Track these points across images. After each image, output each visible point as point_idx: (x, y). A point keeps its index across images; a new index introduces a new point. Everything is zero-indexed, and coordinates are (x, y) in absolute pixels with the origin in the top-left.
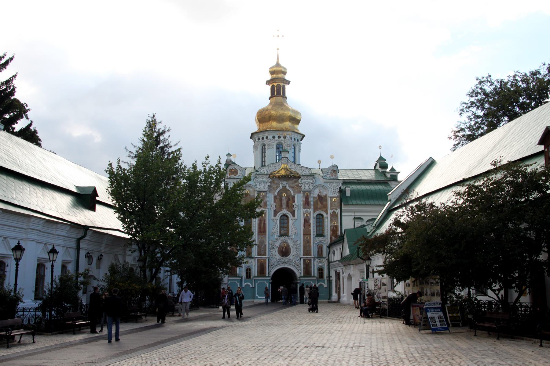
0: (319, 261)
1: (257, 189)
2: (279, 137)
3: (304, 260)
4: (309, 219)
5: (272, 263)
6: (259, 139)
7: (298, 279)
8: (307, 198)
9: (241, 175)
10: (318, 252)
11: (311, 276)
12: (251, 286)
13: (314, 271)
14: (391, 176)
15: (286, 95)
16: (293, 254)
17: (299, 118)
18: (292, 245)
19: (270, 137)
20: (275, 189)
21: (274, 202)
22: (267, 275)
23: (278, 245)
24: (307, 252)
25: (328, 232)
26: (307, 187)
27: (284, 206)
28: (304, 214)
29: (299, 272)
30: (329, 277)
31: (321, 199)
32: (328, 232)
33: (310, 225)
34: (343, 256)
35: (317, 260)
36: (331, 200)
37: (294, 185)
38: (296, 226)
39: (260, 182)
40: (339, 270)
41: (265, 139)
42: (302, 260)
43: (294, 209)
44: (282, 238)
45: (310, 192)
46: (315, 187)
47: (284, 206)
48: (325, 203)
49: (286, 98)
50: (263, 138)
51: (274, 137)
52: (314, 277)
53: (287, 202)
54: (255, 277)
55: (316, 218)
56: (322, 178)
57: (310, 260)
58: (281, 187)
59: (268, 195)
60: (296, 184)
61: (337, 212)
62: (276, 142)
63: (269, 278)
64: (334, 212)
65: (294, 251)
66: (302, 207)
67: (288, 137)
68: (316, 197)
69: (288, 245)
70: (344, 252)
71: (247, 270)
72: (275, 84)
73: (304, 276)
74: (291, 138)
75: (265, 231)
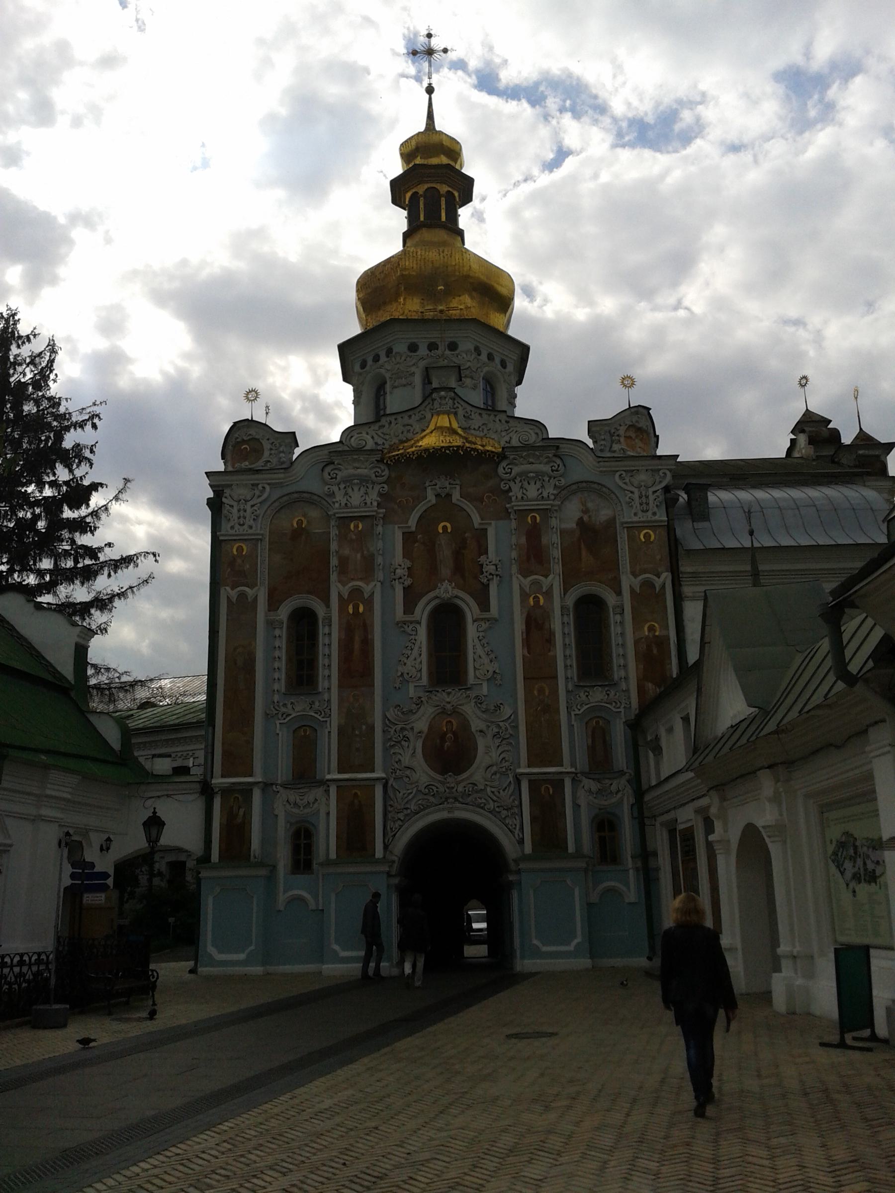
0: (594, 786)
2: (432, 347)
3: (534, 785)
6: (363, 365)
7: (513, 866)
8: (534, 534)
9: (274, 461)
10: (592, 749)
12: (312, 906)
13: (577, 830)
17: (503, 291)
18: (482, 726)
19: (401, 348)
21: (407, 554)
22: (379, 853)
23: (421, 724)
24: (544, 749)
25: (626, 664)
26: (532, 491)
27: (446, 571)
28: (524, 596)
30: (646, 855)
31: (593, 537)
32: (626, 664)
33: (550, 640)
35: (589, 784)
36: (632, 539)
38: (493, 647)
39: (348, 481)
40: (686, 816)
41: (383, 359)
45: (546, 513)
46: (566, 492)
47: (446, 571)
49: (461, 233)
50: (376, 359)
51: (413, 348)
53: (458, 555)
54: (328, 863)
56: (591, 458)
57: (557, 783)
59: (380, 529)
61: (658, 582)
62: (422, 364)
64: (648, 585)
66: (514, 569)
67: (465, 346)
69: (465, 725)
71: (297, 835)
72: (421, 189)
74: (478, 351)
75: (367, 672)
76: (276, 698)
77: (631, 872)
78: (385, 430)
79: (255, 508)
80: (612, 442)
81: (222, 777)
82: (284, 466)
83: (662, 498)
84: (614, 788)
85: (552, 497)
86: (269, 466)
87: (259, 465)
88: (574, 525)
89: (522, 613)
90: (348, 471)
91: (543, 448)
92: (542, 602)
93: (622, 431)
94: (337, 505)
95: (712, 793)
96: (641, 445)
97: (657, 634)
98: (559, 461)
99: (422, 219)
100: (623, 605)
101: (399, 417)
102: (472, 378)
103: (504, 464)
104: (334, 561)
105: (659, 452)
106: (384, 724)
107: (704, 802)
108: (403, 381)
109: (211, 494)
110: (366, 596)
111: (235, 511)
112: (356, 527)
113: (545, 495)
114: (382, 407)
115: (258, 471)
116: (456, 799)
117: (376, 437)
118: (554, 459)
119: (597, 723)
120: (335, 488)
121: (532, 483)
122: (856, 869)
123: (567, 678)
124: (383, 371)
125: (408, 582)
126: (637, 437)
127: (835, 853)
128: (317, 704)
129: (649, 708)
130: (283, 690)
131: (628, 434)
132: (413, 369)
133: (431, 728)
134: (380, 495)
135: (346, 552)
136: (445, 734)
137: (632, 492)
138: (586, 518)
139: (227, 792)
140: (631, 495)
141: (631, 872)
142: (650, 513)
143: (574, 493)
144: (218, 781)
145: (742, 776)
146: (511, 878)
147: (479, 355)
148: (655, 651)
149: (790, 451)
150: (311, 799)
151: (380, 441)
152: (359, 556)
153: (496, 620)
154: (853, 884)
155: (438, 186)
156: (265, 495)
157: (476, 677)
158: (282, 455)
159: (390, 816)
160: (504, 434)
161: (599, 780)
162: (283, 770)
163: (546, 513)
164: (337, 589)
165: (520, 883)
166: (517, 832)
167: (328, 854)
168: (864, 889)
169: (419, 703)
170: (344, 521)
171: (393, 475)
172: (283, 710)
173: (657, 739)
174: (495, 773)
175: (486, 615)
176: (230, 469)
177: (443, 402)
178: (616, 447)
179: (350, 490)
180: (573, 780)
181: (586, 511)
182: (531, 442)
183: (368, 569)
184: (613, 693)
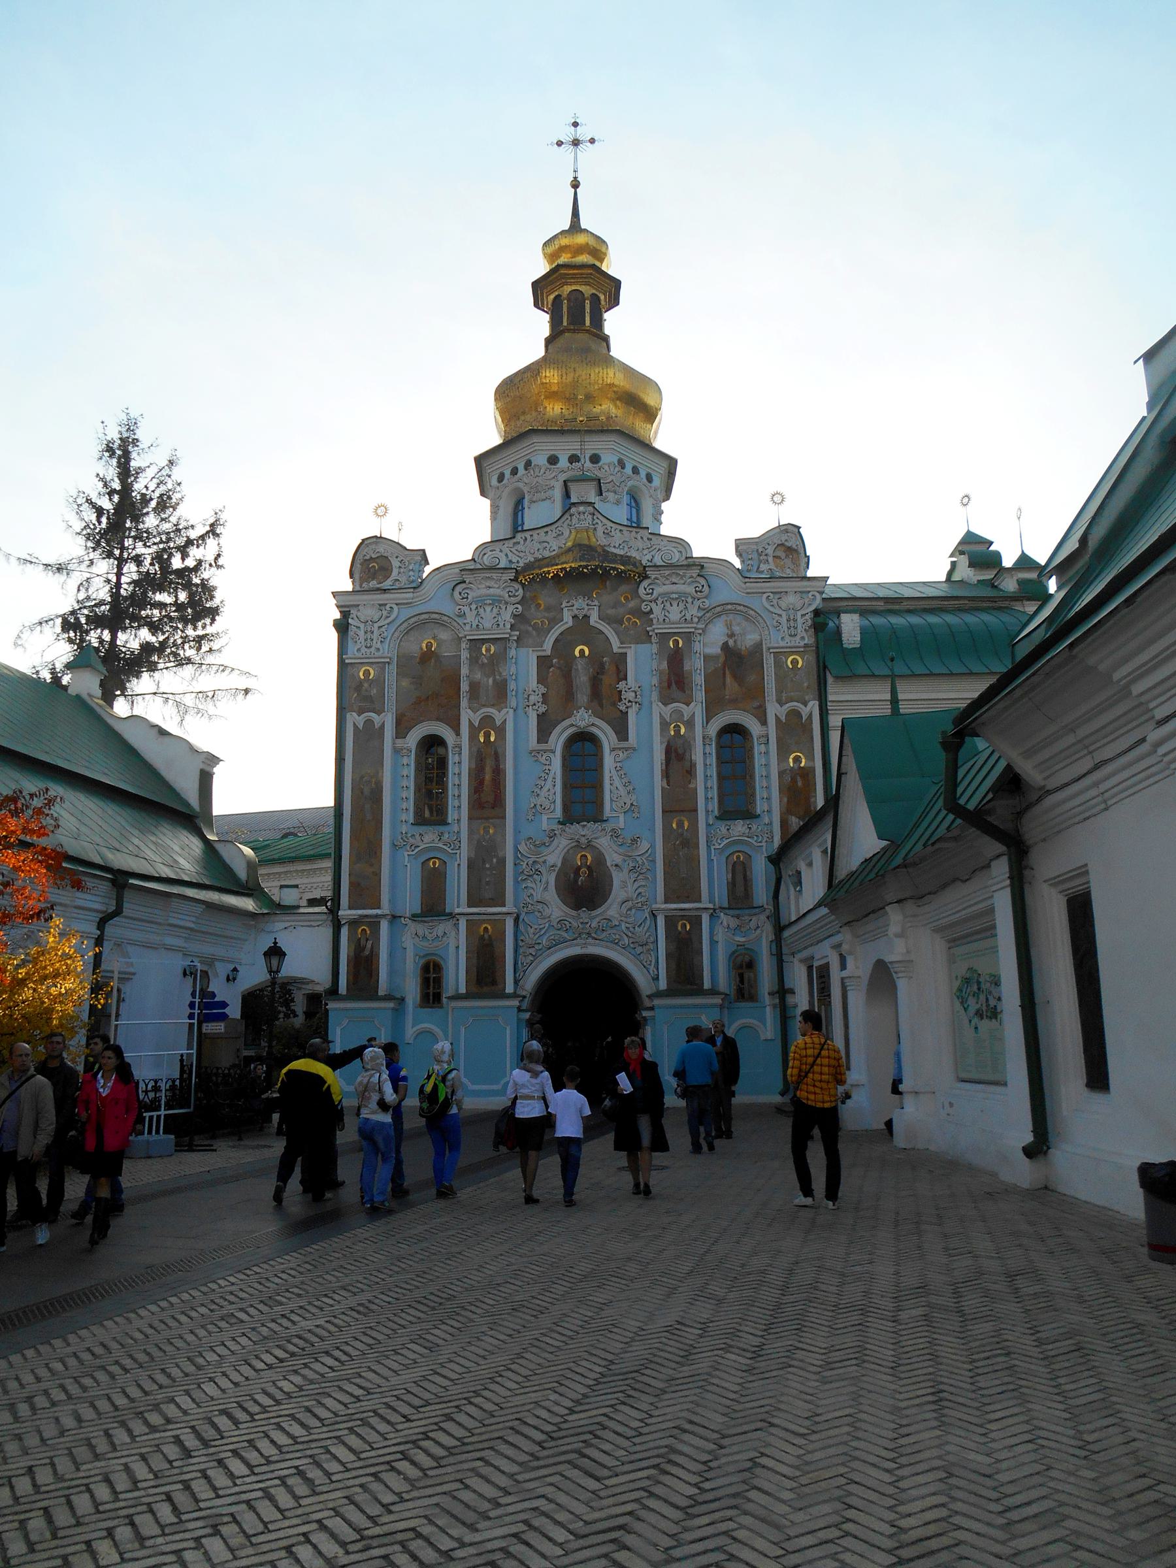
0: (734, 923)
1: (468, 632)
2: (573, 459)
3: (670, 922)
4: (688, 744)
5: (529, 935)
6: (501, 478)
7: (647, 1003)
8: (676, 660)
9: (403, 579)
10: (732, 885)
11: (699, 991)
13: (715, 967)
14: (1021, 582)
15: (608, 329)
16: (623, 895)
18: (618, 859)
20: (543, 632)
21: (541, 681)
22: (509, 989)
23: (554, 856)
24: (682, 883)
26: (675, 613)
27: (582, 697)
28: (665, 725)
29: (647, 972)
30: (782, 992)
31: (738, 664)
33: (690, 772)
34: (841, 873)
36: (778, 664)
37: (621, 610)
38: (631, 776)
39: (481, 603)
40: (824, 952)
42: (661, 921)
43: (623, 708)
44: (575, 829)
45: (688, 637)
46: (711, 614)
48: (752, 678)
49: (606, 339)
50: (515, 471)
51: (553, 460)
52: (713, 992)
53: (595, 682)
54: (457, 997)
55: (720, 747)
56: (738, 579)
57: (696, 922)
58: (568, 620)
59: (512, 653)
60: (632, 604)
61: (804, 711)
63: (515, 1003)
65: (624, 885)
66: (655, 696)
67: (607, 458)
68: (716, 657)
69: (600, 859)
70: (841, 851)
71: (426, 968)
73: (669, 993)
74: (622, 464)
76: (404, 829)
77: (768, 1009)
78: (519, 547)
79: (383, 629)
80: (760, 562)
81: (350, 908)
82: (414, 585)
83: (810, 623)
84: (753, 924)
85: (696, 620)
86: (397, 585)
87: (387, 584)
88: (719, 650)
89: (661, 743)
90: (479, 590)
91: (688, 566)
92: (683, 731)
93: (770, 551)
94: (468, 627)
95: (845, 929)
96: (792, 567)
97: (802, 765)
98: (703, 582)
99: (565, 324)
100: (767, 736)
101: (535, 533)
102: (615, 493)
103: (645, 583)
104: (464, 687)
105: (810, 574)
106: (516, 857)
107: (837, 939)
108: (543, 495)
109: (338, 616)
110: (498, 723)
111: (361, 633)
112: (488, 650)
113: (688, 617)
114: (520, 522)
115: (385, 591)
116: (589, 934)
117: (510, 554)
118: (699, 579)
119: (738, 857)
120: (466, 609)
121: (675, 604)
122: (978, 1006)
123: (707, 811)
124: (521, 485)
125: (543, 709)
126: (787, 556)
127: (960, 990)
128: (446, 835)
129: (792, 842)
130: (412, 821)
131: (778, 553)
132: (553, 483)
133: (565, 860)
134: (515, 616)
135: (478, 676)
136: (579, 868)
137: (780, 615)
138: (731, 643)
139: (354, 923)
140: (777, 618)
141: (768, 1009)
142: (798, 638)
143: (719, 615)
144: (345, 913)
145: (873, 912)
146: (645, 1014)
147: (623, 468)
148: (800, 784)
149: (950, 574)
150: (440, 934)
151: (514, 560)
152: (491, 681)
153: (634, 749)
154: (975, 1020)
155: (583, 288)
156: (393, 616)
157: (612, 810)
158: (411, 573)
159: (521, 950)
160: (645, 552)
161: (738, 917)
162: (411, 901)
163: (688, 637)
164: (468, 716)
165: (653, 1018)
166: (652, 968)
167: (457, 989)
168: (985, 1025)
169: (552, 836)
170: (475, 644)
171: (528, 594)
172: (411, 840)
173: (799, 873)
174: (630, 909)
175: (624, 744)
176: (358, 588)
177: (582, 517)
178: (763, 567)
179: (481, 611)
180: (711, 916)
181: (731, 635)
182: (674, 561)
183: (501, 694)
184: (754, 827)
